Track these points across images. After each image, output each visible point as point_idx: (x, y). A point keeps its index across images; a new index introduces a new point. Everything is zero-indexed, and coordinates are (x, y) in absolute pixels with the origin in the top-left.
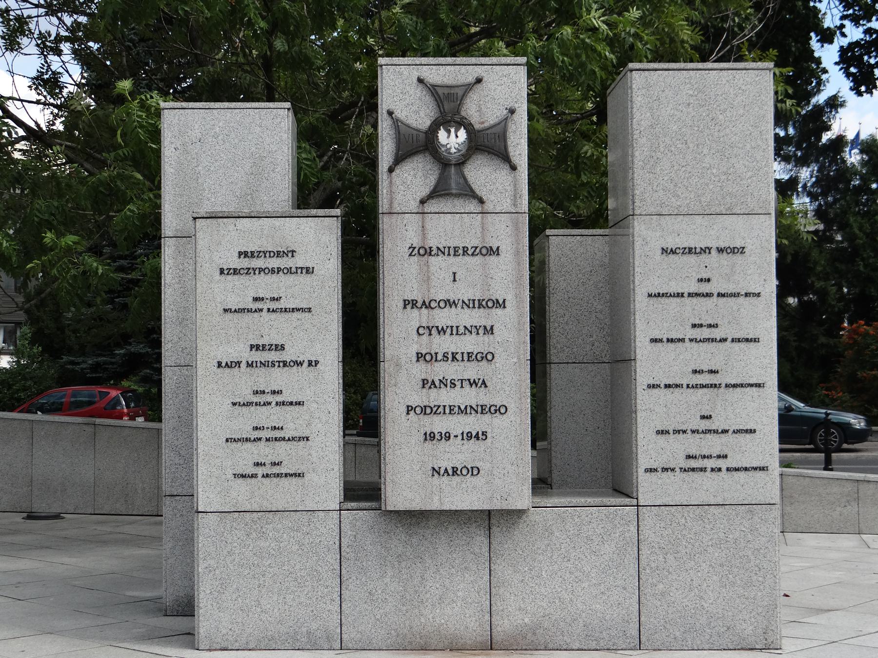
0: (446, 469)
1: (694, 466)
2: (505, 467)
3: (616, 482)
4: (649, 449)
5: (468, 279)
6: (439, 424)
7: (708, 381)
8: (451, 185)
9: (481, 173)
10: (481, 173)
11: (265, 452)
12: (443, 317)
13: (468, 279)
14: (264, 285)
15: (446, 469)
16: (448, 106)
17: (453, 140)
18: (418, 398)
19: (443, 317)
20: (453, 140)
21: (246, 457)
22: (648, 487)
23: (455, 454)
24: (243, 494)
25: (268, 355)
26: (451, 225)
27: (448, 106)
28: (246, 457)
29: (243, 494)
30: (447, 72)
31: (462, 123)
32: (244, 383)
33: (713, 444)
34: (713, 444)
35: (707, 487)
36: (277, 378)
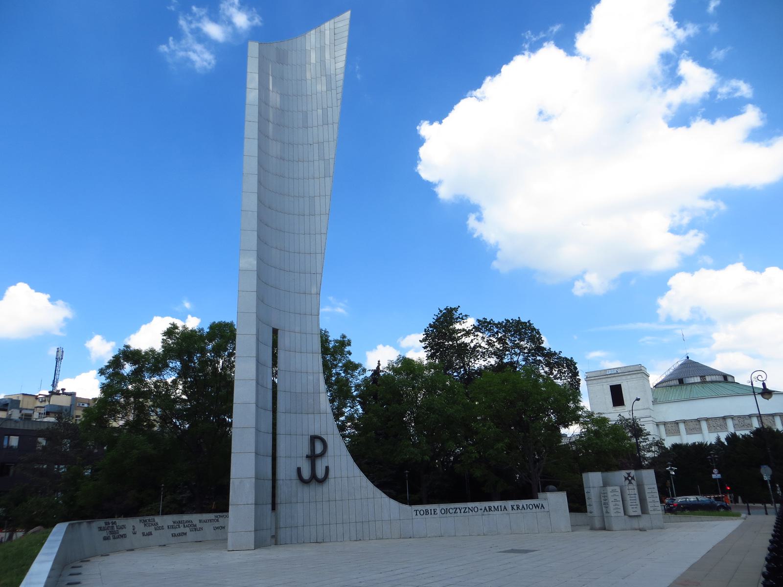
0: (485, 508)
1: (654, 510)
2: (639, 512)
3: (648, 513)
4: (650, 509)
5: (632, 492)
6: (633, 507)
7: (654, 502)
8: (630, 483)
9: (633, 481)
10: (633, 481)
11: (617, 510)
12: (632, 496)
13: (632, 492)
14: (615, 493)
15: (485, 508)
16: (629, 474)
17: (630, 478)
18: (631, 504)
19: (632, 496)
20: (630, 478)
21: (615, 511)
22: (651, 513)
23: (634, 510)
24: (616, 515)
25: (616, 500)
26: (631, 487)
27: (629, 474)
28: (615, 511)
29: (616, 515)
30: (628, 471)
31: (630, 477)
32: (614, 503)
33: (655, 508)
34: (655, 508)
35: (656, 512)
36: (616, 503)
